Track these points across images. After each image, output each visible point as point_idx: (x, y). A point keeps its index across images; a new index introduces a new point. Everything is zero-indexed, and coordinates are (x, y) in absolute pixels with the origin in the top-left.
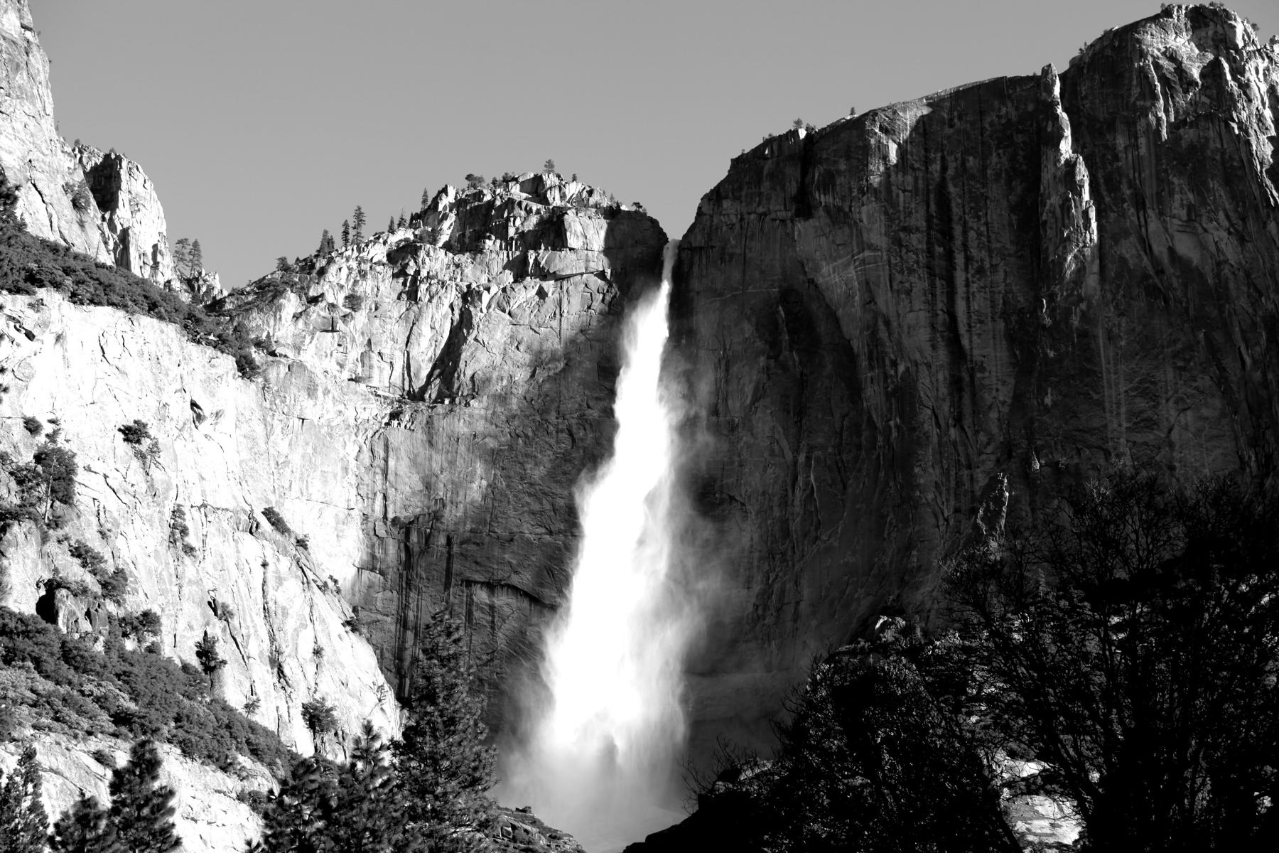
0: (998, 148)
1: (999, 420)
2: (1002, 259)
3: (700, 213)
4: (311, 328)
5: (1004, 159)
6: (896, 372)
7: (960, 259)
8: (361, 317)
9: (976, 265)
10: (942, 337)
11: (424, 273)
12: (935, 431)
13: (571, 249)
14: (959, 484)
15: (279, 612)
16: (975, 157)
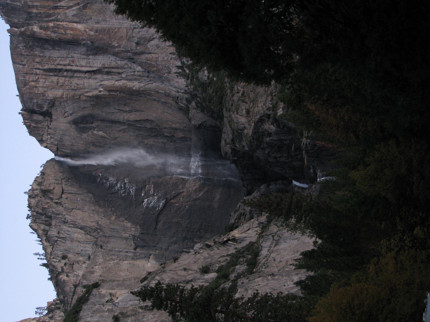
0: (33, 51)
1: (121, 61)
2: (70, 54)
3: (46, 147)
4: (71, 271)
5: (37, 49)
6: (103, 91)
7: (69, 68)
8: (70, 255)
9: (71, 63)
10: (93, 76)
11: (57, 235)
12: (122, 81)
13: (54, 188)
14: (140, 76)
15: (172, 280)
16: (36, 59)
